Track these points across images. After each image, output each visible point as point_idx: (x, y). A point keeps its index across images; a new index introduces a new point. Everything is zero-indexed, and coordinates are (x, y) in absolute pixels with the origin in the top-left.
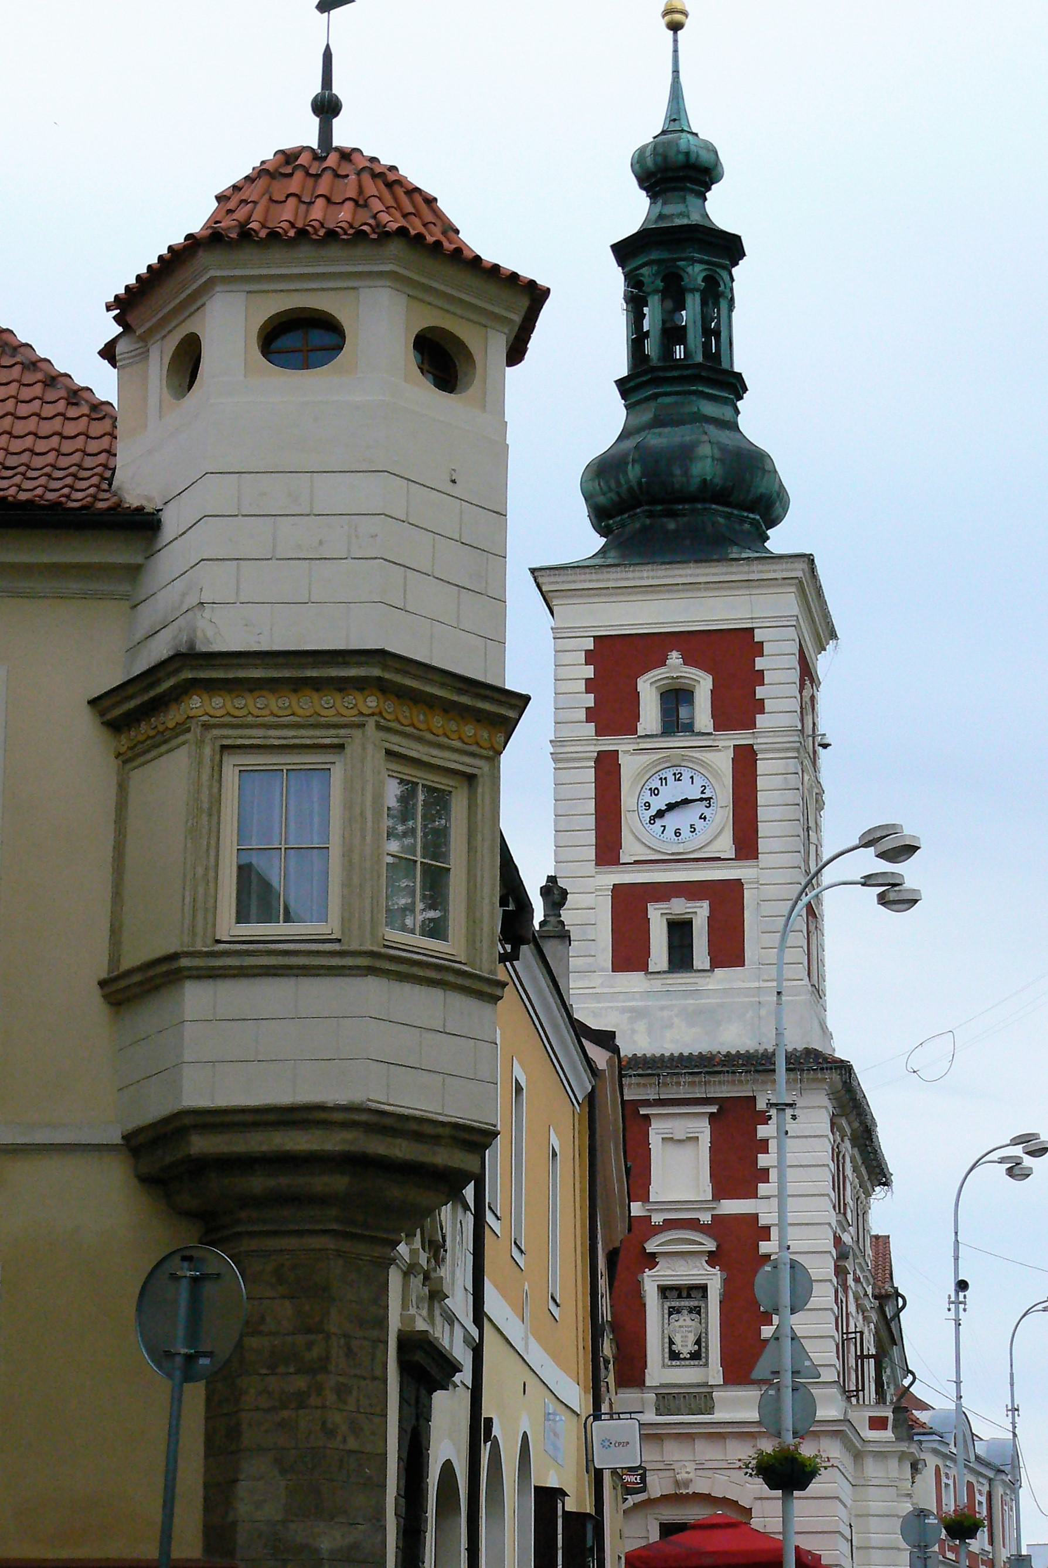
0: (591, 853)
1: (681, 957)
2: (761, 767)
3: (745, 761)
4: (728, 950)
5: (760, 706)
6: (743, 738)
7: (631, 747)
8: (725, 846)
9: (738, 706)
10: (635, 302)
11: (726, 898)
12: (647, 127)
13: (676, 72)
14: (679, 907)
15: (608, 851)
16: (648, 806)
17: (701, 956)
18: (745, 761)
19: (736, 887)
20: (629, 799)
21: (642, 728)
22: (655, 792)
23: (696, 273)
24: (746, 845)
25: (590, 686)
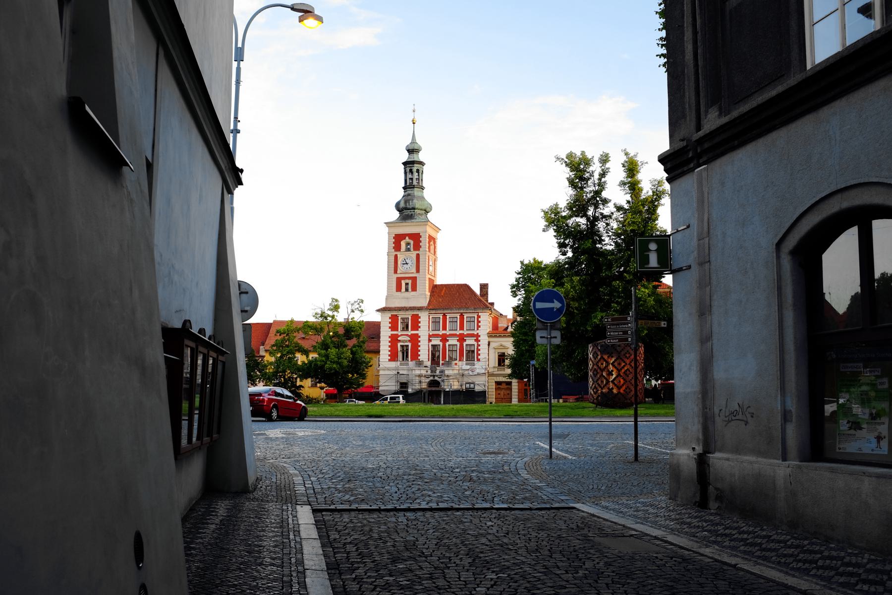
1: (407, 290)
4: (414, 289)
6: (417, 252)
8: (414, 270)
9: (417, 247)
10: (406, 173)
11: (414, 279)
12: (408, 141)
14: (407, 281)
15: (396, 272)
17: (410, 289)
23: (415, 169)
24: (418, 271)
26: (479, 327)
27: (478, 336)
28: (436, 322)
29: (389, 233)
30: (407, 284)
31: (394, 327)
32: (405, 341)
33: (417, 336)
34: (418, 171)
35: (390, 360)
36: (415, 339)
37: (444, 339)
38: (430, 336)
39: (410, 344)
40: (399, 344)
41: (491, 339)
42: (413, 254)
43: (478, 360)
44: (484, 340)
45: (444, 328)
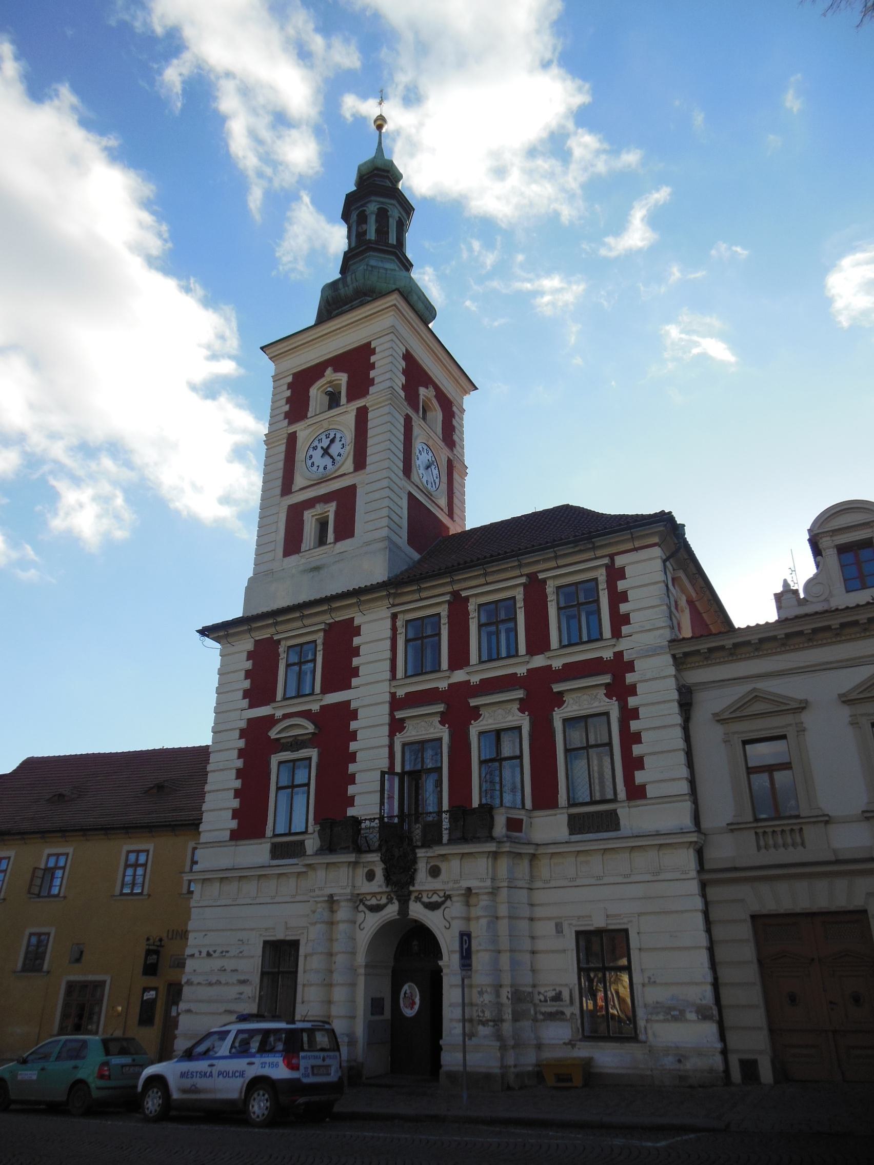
0: (278, 491)
1: (322, 540)
2: (370, 415)
3: (362, 416)
4: (345, 529)
5: (371, 382)
6: (360, 403)
7: (303, 427)
8: (349, 466)
9: (360, 385)
11: (345, 499)
13: (380, 143)
14: (319, 509)
15: (287, 488)
16: (311, 457)
17: (331, 536)
18: (362, 416)
19: (352, 489)
20: (300, 455)
21: (309, 415)
22: (315, 448)
24: (360, 463)
25: (289, 400)
26: (620, 621)
27: (620, 666)
28: (421, 636)
29: (276, 379)
30: (323, 525)
31: (260, 687)
32: (296, 744)
33: (345, 713)
34: (382, 215)
35: (236, 836)
36: (334, 729)
37: (458, 708)
38: (396, 703)
39: (314, 753)
40: (275, 760)
41: (695, 676)
42: (345, 419)
43: (636, 793)
44: (655, 685)
45: (459, 659)
